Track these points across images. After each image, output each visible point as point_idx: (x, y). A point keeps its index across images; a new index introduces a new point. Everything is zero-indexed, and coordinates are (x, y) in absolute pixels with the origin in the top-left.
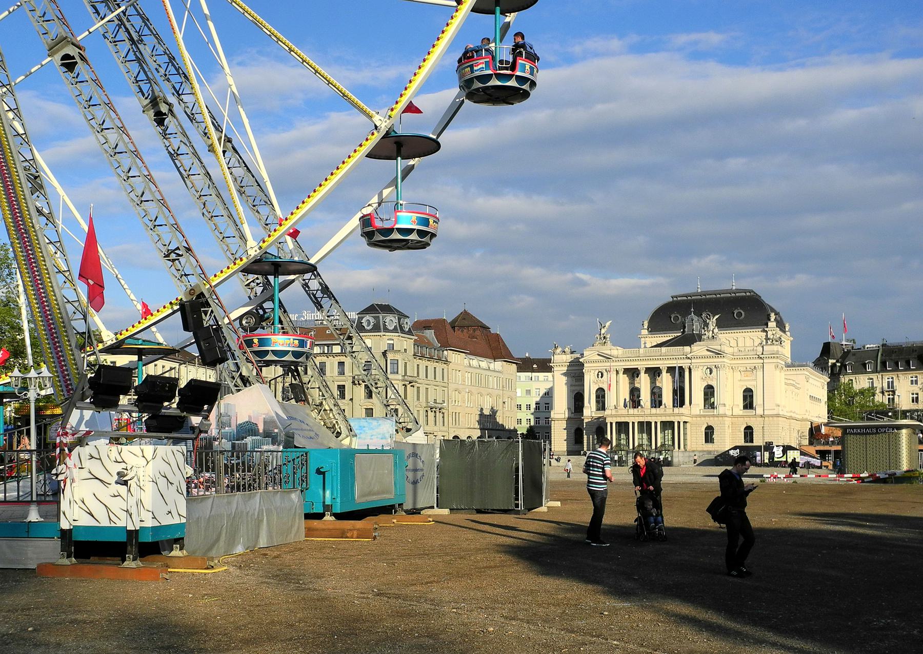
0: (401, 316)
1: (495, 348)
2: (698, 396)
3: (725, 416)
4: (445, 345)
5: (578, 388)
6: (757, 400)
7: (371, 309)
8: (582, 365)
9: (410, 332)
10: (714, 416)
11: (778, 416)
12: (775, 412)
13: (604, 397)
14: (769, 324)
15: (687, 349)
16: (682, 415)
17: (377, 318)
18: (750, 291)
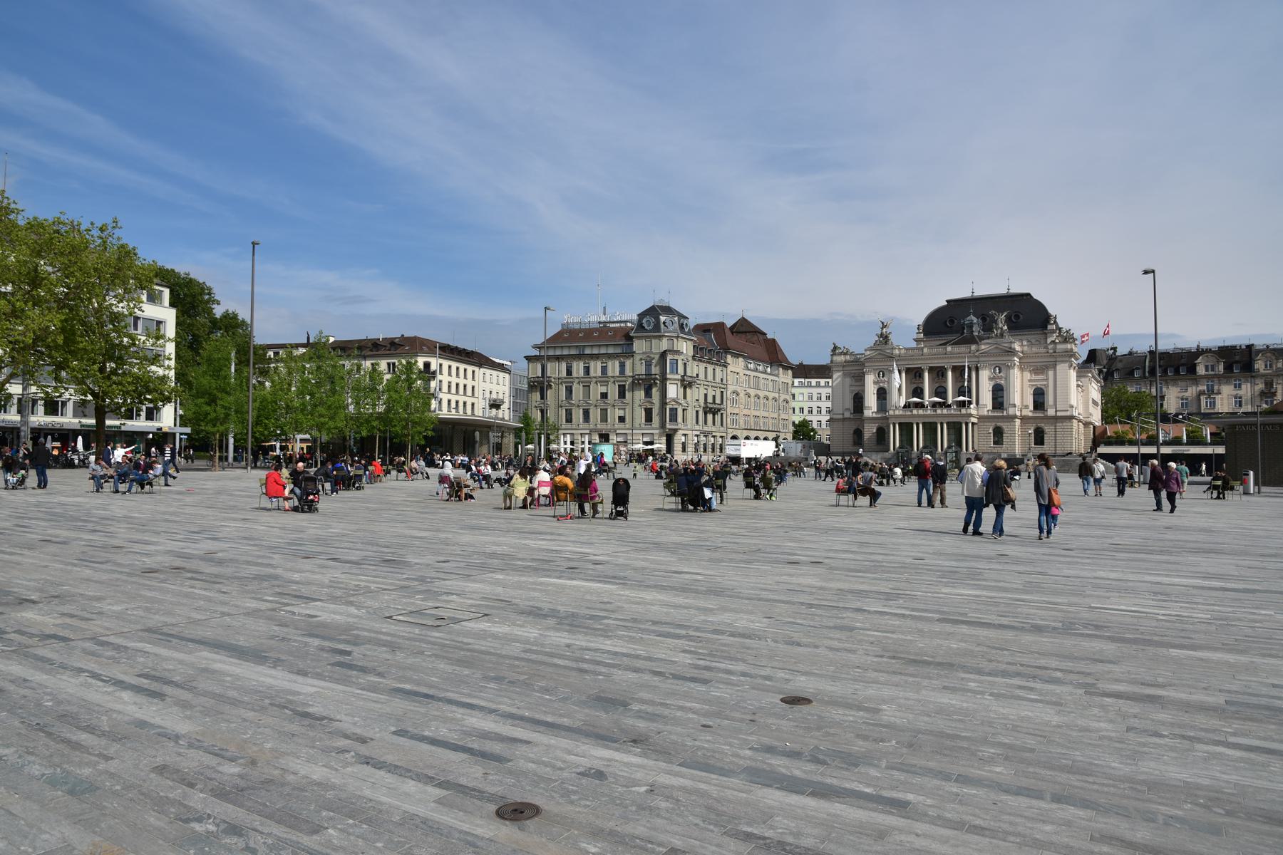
0: (681, 316)
1: (771, 354)
2: (987, 398)
3: (1015, 417)
4: (726, 350)
5: (856, 389)
6: (1050, 399)
7: (654, 312)
8: (863, 364)
9: (689, 333)
10: (1003, 417)
11: (1072, 417)
12: (1068, 414)
13: (885, 399)
14: (1049, 327)
15: (973, 347)
16: (971, 415)
17: (658, 320)
18: (1029, 295)
